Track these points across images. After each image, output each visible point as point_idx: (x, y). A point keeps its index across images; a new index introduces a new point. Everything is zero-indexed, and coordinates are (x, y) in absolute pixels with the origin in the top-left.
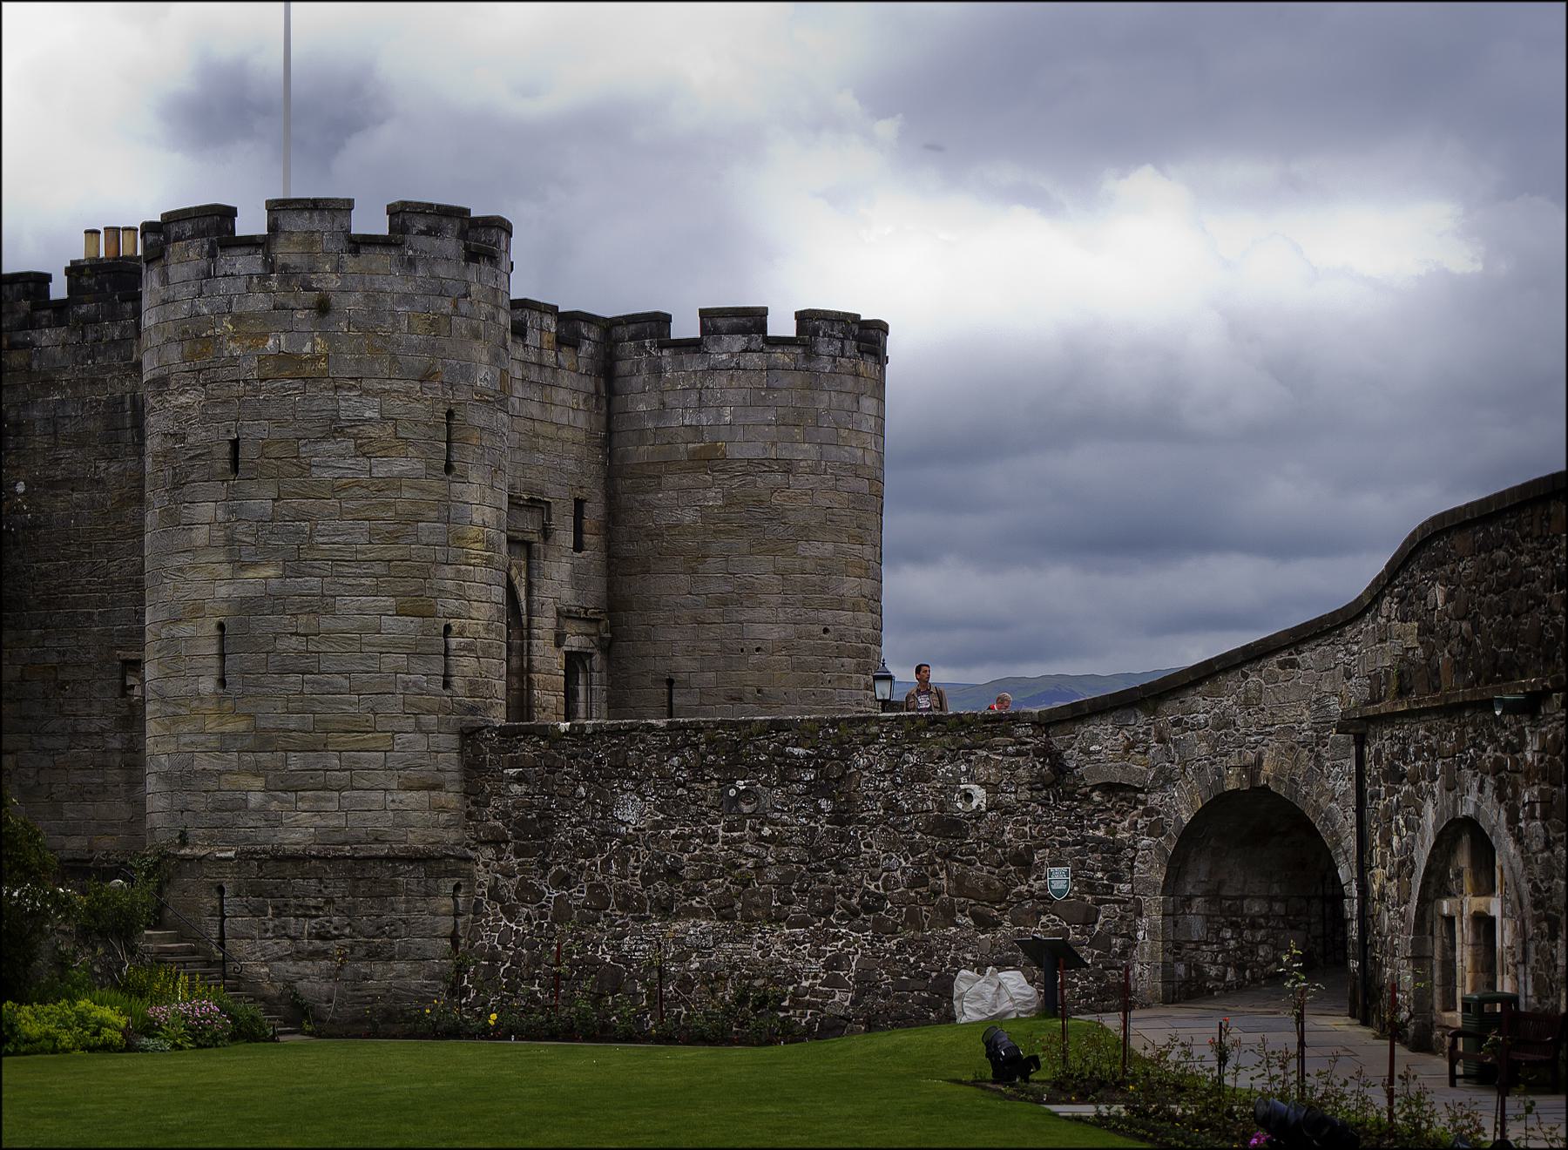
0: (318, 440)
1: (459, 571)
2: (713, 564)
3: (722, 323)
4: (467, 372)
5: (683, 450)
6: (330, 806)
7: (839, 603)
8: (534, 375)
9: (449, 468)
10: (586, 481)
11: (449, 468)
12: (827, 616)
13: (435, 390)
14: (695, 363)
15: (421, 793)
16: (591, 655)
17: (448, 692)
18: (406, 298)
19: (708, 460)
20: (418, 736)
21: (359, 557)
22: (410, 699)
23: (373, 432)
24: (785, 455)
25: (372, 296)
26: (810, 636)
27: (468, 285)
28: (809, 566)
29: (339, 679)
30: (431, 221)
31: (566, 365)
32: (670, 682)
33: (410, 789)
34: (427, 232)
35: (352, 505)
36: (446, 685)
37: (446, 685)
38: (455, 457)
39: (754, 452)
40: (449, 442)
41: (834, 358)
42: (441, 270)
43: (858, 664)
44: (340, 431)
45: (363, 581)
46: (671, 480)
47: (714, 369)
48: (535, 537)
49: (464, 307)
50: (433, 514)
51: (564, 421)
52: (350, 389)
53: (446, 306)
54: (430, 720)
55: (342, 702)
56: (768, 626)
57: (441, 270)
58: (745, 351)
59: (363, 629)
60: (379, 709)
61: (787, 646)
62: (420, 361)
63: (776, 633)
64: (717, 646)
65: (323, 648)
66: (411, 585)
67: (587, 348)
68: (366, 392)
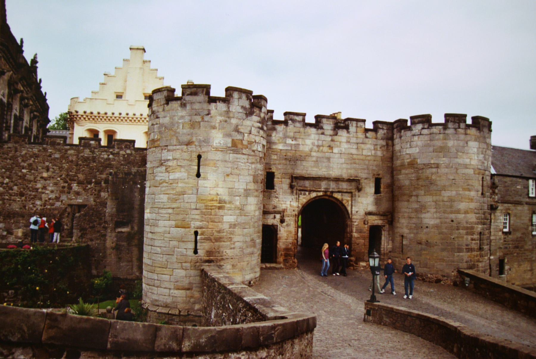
0: (158, 167)
1: (202, 212)
2: (414, 198)
3: (416, 120)
4: (207, 141)
5: (407, 161)
6: (156, 292)
7: (458, 212)
8: (354, 140)
9: (198, 175)
10: (380, 172)
11: (198, 175)
12: (453, 216)
13: (192, 148)
14: (409, 133)
15: (183, 291)
16: (384, 226)
17: (196, 255)
18: (182, 117)
19: (412, 164)
20: (182, 271)
21: (165, 207)
22: (179, 257)
23: (170, 163)
24: (436, 162)
25: (172, 118)
26: (446, 223)
27: (209, 110)
28: (445, 199)
29: (158, 249)
30: (194, 90)
31: (371, 137)
32: (402, 236)
33: (178, 289)
34: (191, 94)
35: (163, 189)
36: (196, 252)
37: (196, 252)
38: (201, 171)
39: (426, 161)
40: (199, 166)
41: (455, 129)
42: (197, 106)
43: (467, 232)
44: (162, 165)
45: (165, 215)
46: (403, 171)
47: (414, 135)
48: (353, 191)
49: (207, 118)
50: (190, 192)
51: (369, 154)
52: (165, 149)
53: (198, 118)
54: (188, 265)
55: (159, 257)
56: (430, 219)
57: (197, 106)
58: (423, 129)
59: (165, 232)
60: (168, 260)
61: (437, 226)
62: (186, 139)
63: (432, 222)
64: (414, 225)
65: (155, 238)
66: (180, 217)
67: (381, 133)
68: (168, 151)
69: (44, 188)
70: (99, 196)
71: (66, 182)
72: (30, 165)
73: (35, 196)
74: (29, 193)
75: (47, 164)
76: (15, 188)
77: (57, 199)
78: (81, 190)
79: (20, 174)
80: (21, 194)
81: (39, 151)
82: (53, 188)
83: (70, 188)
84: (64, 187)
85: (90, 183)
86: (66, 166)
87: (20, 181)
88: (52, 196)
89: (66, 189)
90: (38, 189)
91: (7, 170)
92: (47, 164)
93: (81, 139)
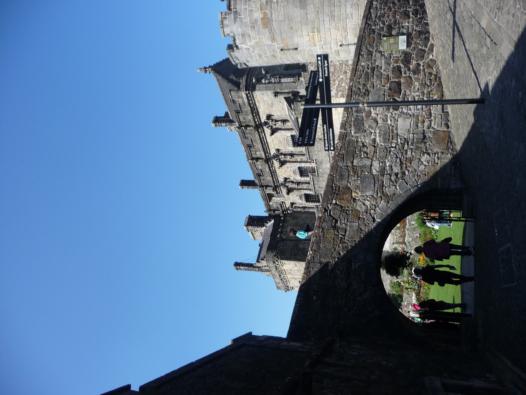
73: (345, 65)
74: (344, 68)
76: (341, 77)
87: (336, 75)
90: (340, 64)
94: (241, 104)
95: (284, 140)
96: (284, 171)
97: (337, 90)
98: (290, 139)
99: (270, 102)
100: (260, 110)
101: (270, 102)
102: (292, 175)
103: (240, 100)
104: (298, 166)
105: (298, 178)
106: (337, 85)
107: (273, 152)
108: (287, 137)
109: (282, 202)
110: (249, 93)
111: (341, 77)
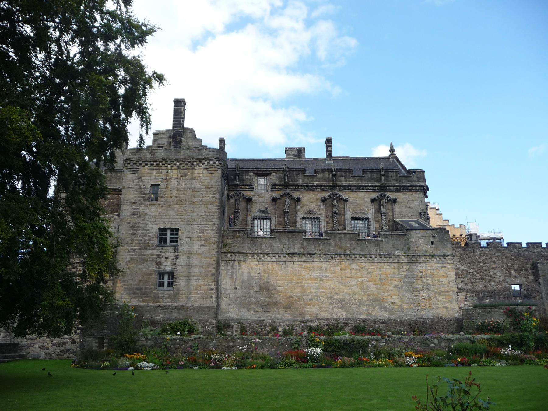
69: (495, 274)
70: (528, 278)
71: (507, 270)
72: (484, 261)
75: (494, 259)
76: (478, 275)
77: (504, 281)
78: (517, 275)
79: (479, 266)
80: (482, 279)
81: (488, 252)
82: (500, 274)
83: (510, 274)
84: (506, 273)
85: (522, 270)
86: (505, 260)
88: (501, 279)
89: (508, 275)
91: (471, 264)
92: (494, 259)
93: (508, 244)
94: (410, 179)
95: (361, 210)
96: (312, 200)
97: (463, 270)
98: (363, 216)
99: (412, 205)
100: (401, 194)
101: (412, 205)
102: (306, 208)
103: (416, 179)
104: (323, 218)
105: (301, 216)
106: (469, 270)
107: (344, 195)
108: (366, 214)
109: (253, 188)
110: (424, 189)
111: (478, 275)
